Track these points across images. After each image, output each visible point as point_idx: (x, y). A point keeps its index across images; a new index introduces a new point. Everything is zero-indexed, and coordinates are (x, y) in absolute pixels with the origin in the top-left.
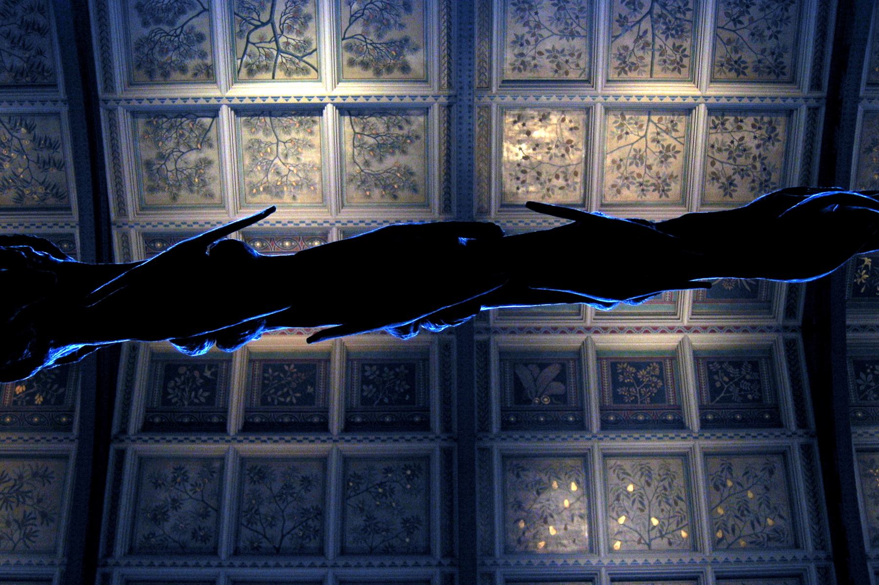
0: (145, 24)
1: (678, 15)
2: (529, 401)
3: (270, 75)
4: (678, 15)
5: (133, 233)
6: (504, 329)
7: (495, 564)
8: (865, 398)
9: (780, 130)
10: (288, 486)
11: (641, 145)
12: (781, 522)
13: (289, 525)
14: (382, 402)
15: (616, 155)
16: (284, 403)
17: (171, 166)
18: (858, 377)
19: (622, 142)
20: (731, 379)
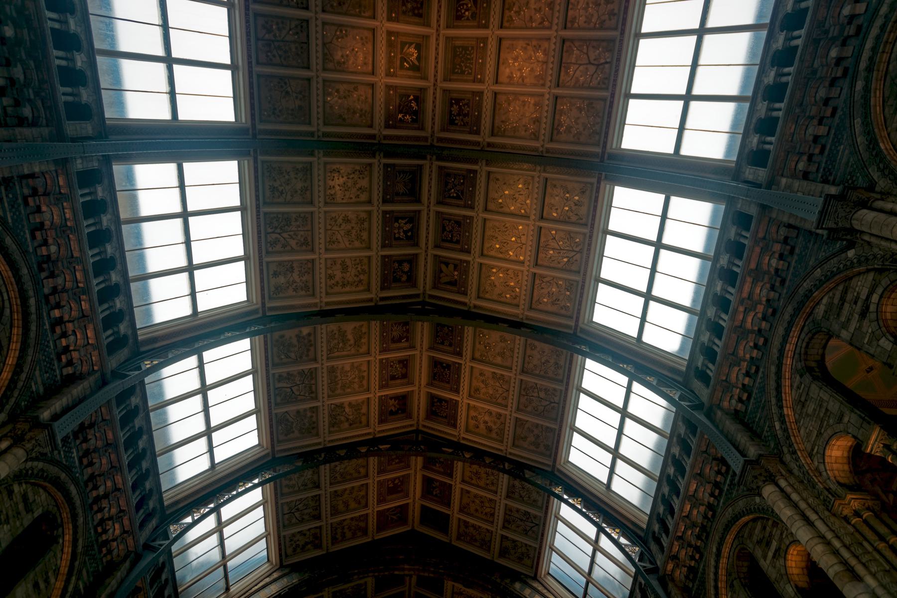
0: (293, 432)
2: (456, 280)
3: (314, 387)
5: (378, 429)
7: (523, 314)
8: (467, 123)
9: (334, 167)
10: (483, 382)
11: (342, 233)
12: (521, 181)
13: (498, 384)
14: (452, 339)
15: (347, 244)
17: (351, 417)
18: (457, 124)
20: (453, 188)
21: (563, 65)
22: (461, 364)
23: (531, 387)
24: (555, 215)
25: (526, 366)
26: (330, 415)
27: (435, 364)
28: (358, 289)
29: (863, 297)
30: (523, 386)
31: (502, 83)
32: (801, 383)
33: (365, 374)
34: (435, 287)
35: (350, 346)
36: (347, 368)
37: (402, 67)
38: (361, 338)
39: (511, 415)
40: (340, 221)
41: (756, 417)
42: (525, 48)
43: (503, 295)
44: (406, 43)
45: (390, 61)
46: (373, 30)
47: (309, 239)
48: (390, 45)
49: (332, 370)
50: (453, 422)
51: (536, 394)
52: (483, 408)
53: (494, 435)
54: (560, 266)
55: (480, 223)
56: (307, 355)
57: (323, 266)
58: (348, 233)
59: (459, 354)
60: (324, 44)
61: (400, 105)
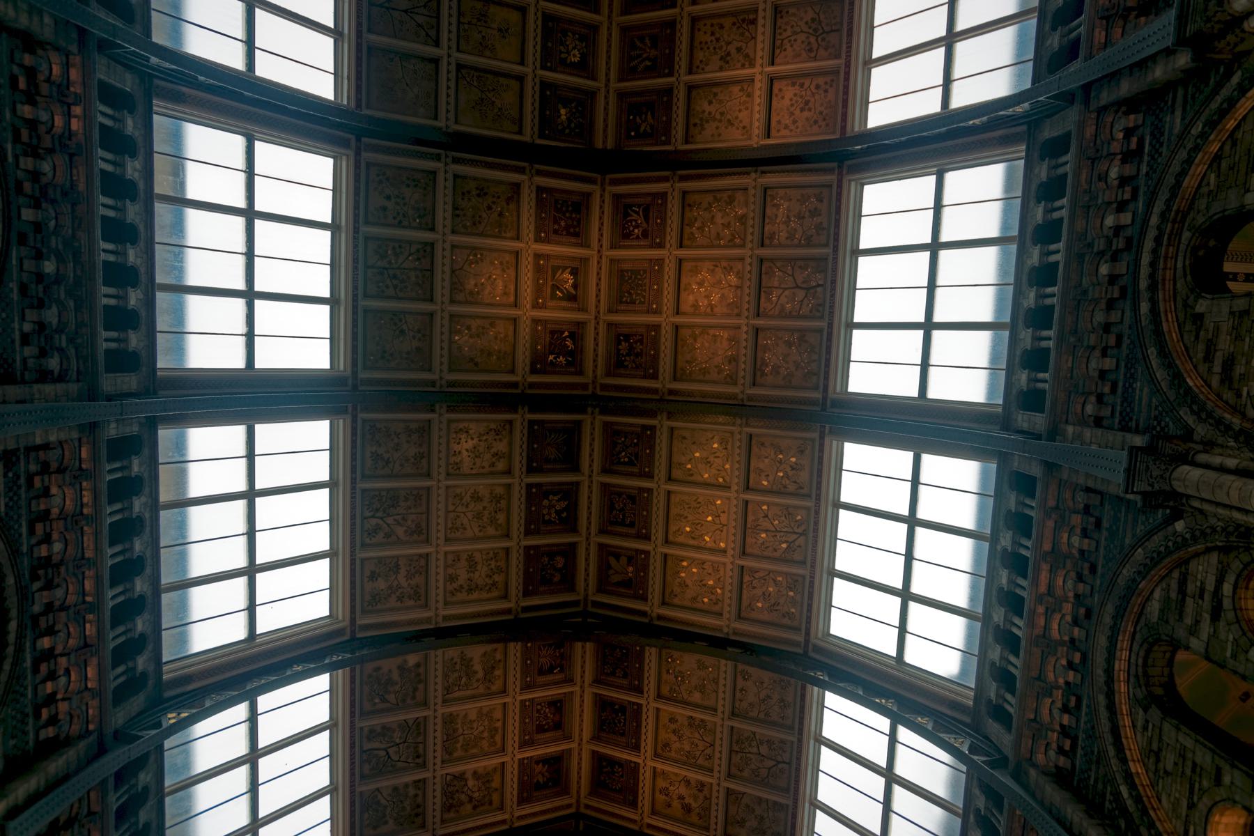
0: (386, 823)
1: (384, 499)
2: (630, 579)
3: (421, 746)
4: (384, 499)
5: (517, 814)
6: (585, 590)
7: (728, 626)
9: (461, 426)
10: (674, 732)
11: (470, 515)
13: (697, 735)
15: (476, 530)
16: (625, 723)
17: (476, 795)
18: (627, 366)
19: (468, 527)
20: (623, 451)
21: (763, 290)
22: (641, 705)
23: (747, 739)
24: (765, 483)
25: (737, 705)
26: (444, 794)
27: (602, 705)
28: (490, 595)
29: (1210, 587)
30: (735, 737)
31: (685, 314)
32: (1147, 721)
33: (499, 724)
34: (600, 590)
35: (478, 681)
36: (473, 716)
37: (553, 297)
38: (493, 668)
39: (719, 785)
40: (467, 498)
41: (1089, 777)
42: (713, 271)
43: (699, 599)
44: (558, 268)
45: (538, 290)
46: (517, 254)
47: (424, 525)
48: (539, 270)
49: (449, 720)
50: (631, 798)
51: (755, 750)
52: (676, 775)
53: (694, 818)
54: (777, 554)
55: (662, 498)
56: (414, 698)
57: (441, 563)
58: (479, 516)
59: (639, 690)
60: (453, 272)
61: (551, 344)
